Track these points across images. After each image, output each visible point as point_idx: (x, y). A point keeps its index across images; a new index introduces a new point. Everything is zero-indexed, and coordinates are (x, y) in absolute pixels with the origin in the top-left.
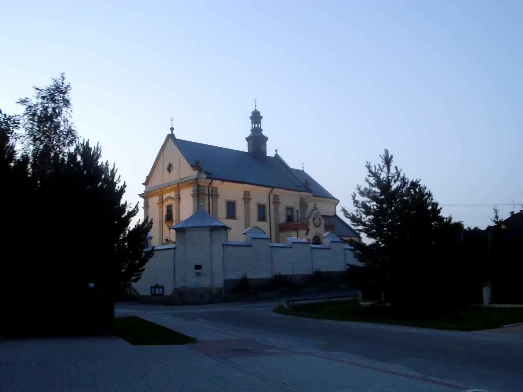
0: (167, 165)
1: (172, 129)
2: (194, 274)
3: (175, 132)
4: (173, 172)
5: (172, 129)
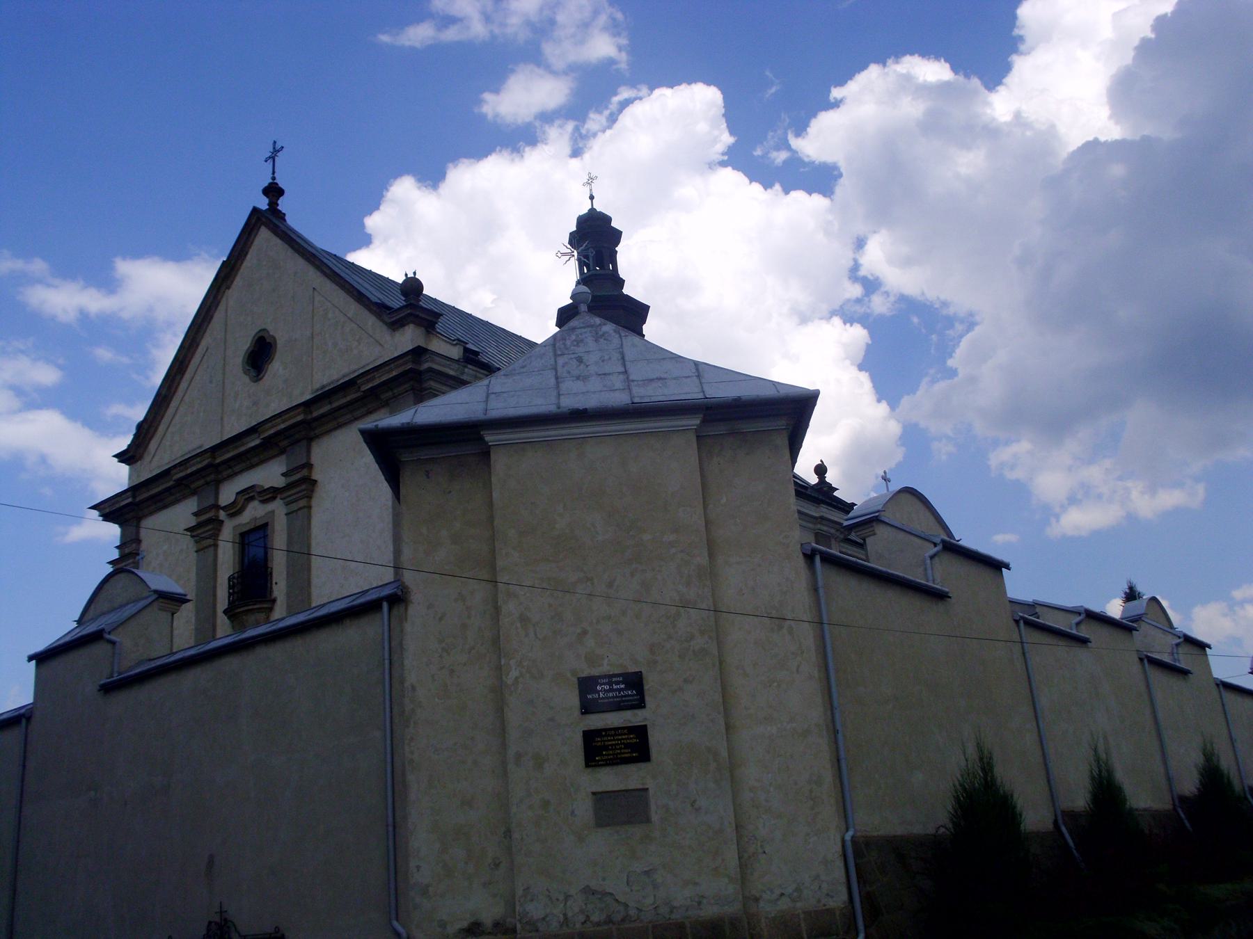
0: (243, 344)
1: (273, 191)
2: (584, 808)
3: (283, 204)
4: (276, 368)
5: (273, 191)
